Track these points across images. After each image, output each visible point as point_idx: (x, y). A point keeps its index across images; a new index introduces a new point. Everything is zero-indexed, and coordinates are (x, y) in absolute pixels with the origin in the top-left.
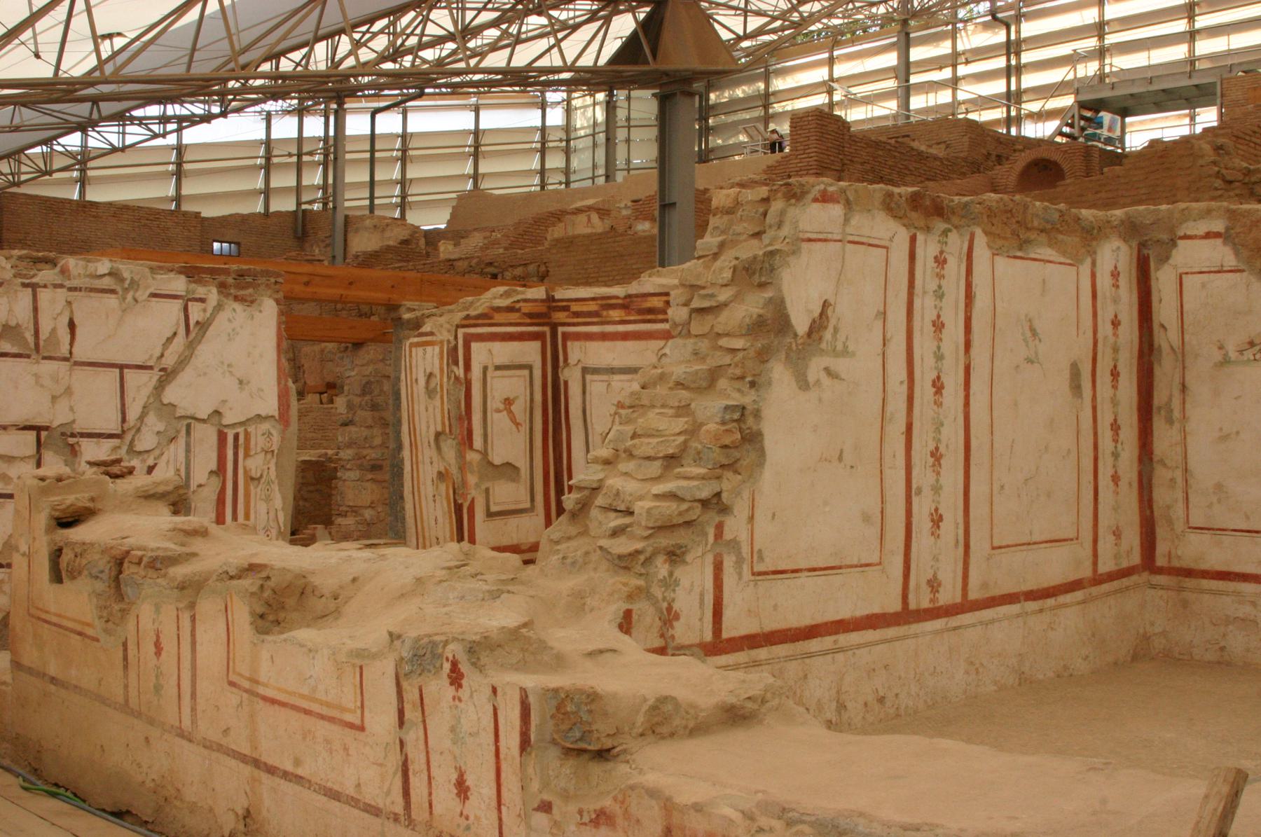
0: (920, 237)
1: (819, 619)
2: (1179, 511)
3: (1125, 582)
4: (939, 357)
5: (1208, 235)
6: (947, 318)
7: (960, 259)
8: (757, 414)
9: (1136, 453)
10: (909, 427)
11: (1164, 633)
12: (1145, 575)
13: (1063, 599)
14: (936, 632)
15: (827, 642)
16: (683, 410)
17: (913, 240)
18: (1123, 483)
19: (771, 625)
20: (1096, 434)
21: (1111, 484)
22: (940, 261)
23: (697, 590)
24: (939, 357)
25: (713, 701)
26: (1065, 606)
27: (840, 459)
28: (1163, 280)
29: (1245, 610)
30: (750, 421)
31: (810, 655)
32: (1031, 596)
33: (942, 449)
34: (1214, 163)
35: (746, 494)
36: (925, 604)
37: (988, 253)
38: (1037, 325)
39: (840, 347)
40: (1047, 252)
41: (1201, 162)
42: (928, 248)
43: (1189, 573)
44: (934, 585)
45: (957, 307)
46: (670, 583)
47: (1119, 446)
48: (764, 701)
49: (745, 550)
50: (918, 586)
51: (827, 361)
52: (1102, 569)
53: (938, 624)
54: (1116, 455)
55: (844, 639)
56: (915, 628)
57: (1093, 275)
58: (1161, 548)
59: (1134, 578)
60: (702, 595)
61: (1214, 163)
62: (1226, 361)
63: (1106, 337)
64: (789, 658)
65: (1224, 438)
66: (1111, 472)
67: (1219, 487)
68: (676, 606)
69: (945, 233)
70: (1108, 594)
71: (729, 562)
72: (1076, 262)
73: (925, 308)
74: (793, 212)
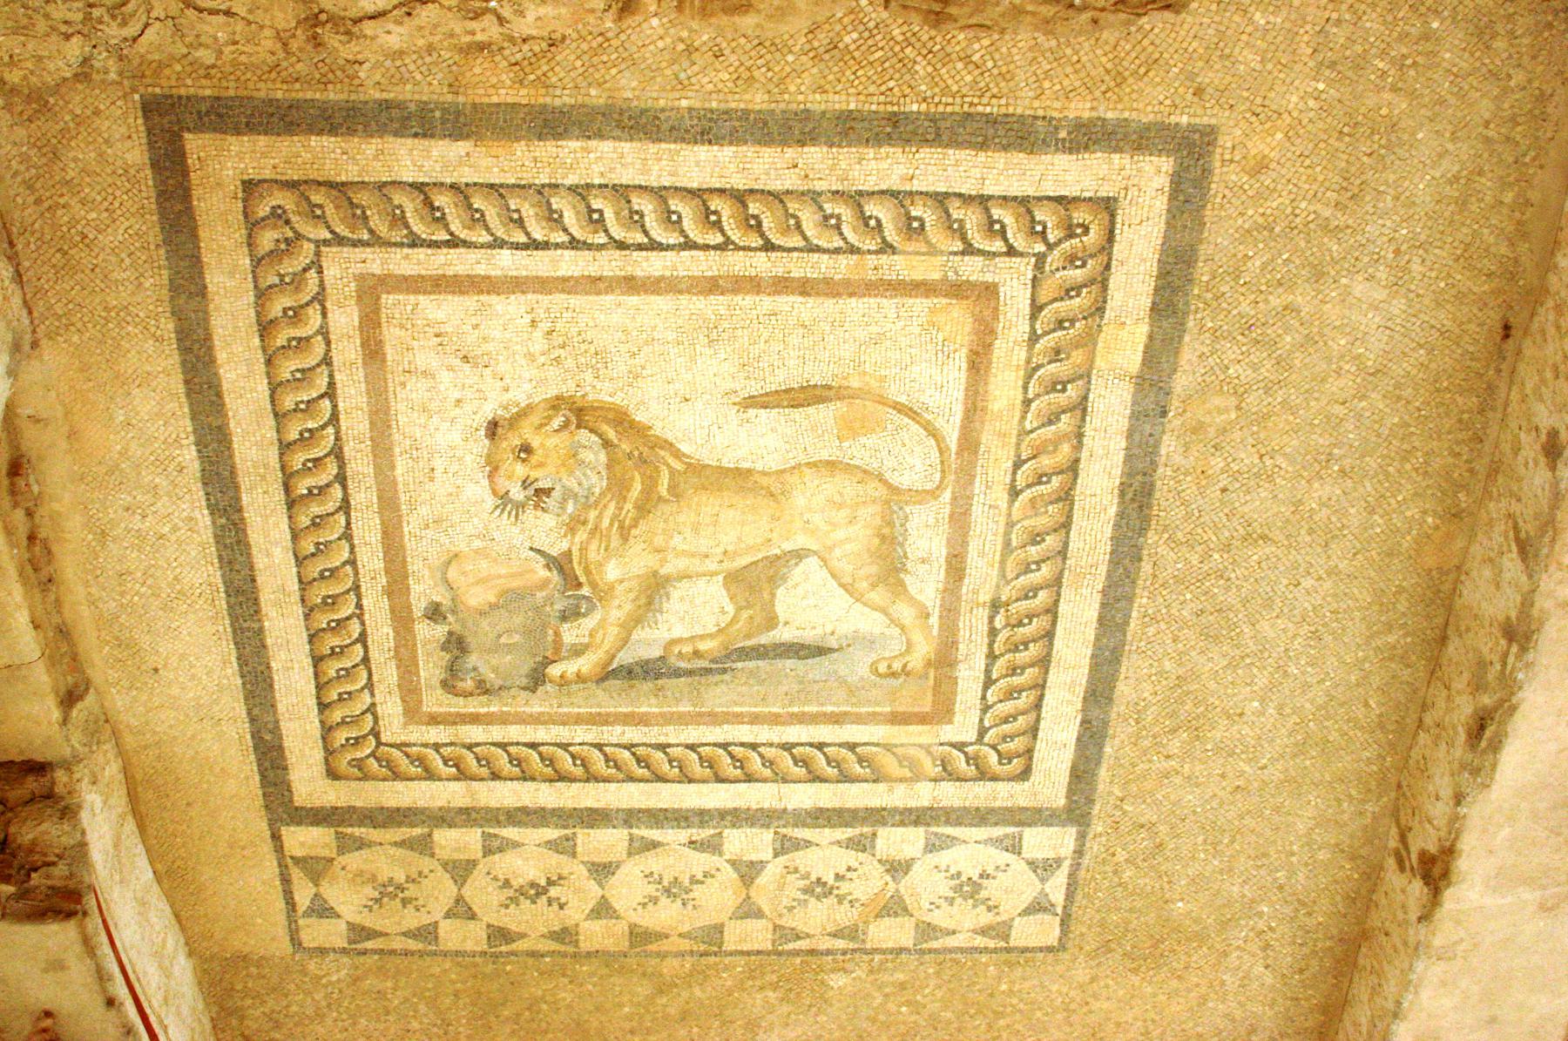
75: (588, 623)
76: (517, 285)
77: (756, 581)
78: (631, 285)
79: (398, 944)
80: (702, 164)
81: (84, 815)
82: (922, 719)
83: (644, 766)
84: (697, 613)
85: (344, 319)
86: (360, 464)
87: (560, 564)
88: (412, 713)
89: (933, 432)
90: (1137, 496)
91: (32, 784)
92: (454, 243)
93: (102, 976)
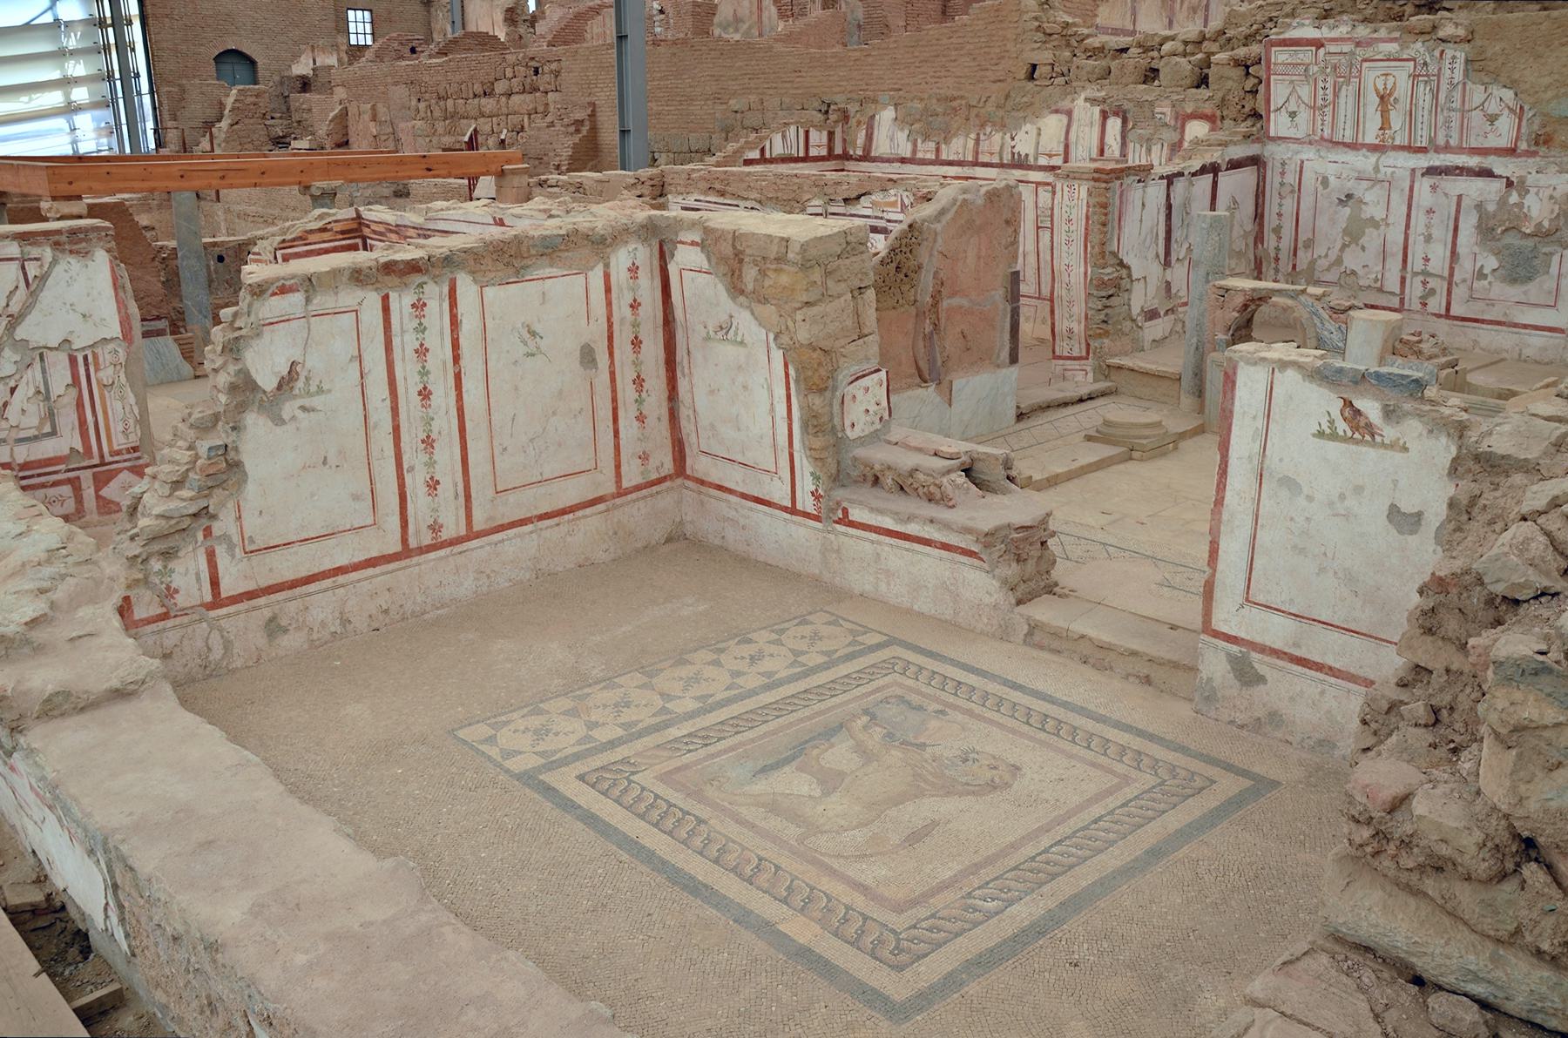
0: (393, 296)
1: (316, 571)
2: (693, 438)
3: (655, 489)
4: (424, 373)
5: (693, 243)
6: (432, 340)
7: (441, 299)
8: (236, 449)
9: (666, 394)
10: (396, 429)
11: (692, 522)
12: (679, 481)
13: (580, 513)
14: (441, 558)
15: (328, 583)
16: (190, 448)
17: (386, 298)
18: (651, 421)
19: (264, 583)
20: (614, 391)
21: (636, 424)
22: (419, 306)
23: (192, 572)
24: (424, 373)
25: (106, 686)
26: (585, 517)
27: (325, 463)
28: (673, 269)
29: (732, 514)
30: (232, 454)
31: (310, 595)
32: (541, 517)
33: (434, 436)
34: (1036, 19)
35: (231, 504)
36: (427, 540)
37: (475, 288)
38: (537, 328)
39: (313, 389)
40: (548, 271)
41: (1026, 17)
42: (402, 303)
43: (702, 482)
44: (435, 528)
45: (442, 333)
46: (166, 572)
47: (644, 394)
48: (143, 682)
49: (236, 539)
50: (417, 532)
51: (300, 402)
52: (626, 484)
53: (442, 553)
54: (639, 401)
55: (341, 579)
56: (415, 560)
57: (607, 277)
58: (689, 462)
59: (668, 484)
60: (198, 575)
61: (1036, 19)
62: (708, 338)
63: (622, 320)
64: (286, 600)
65: (712, 392)
66: (633, 413)
67: (712, 426)
68: (173, 586)
69: (421, 286)
70: (638, 500)
71: (221, 551)
72: (584, 271)
73: (406, 342)
74: (256, 305)
75: (877, 737)
76: (1080, 808)
77: (830, 781)
78: (1046, 829)
79: (786, 625)
80: (1085, 877)
81: (996, 584)
82: (670, 772)
83: (779, 708)
84: (839, 755)
85: (1120, 768)
86: (1043, 736)
87: (922, 746)
88: (900, 685)
89: (839, 856)
90: (694, 888)
91: (1019, 594)
92: (1123, 805)
93: (947, 526)
